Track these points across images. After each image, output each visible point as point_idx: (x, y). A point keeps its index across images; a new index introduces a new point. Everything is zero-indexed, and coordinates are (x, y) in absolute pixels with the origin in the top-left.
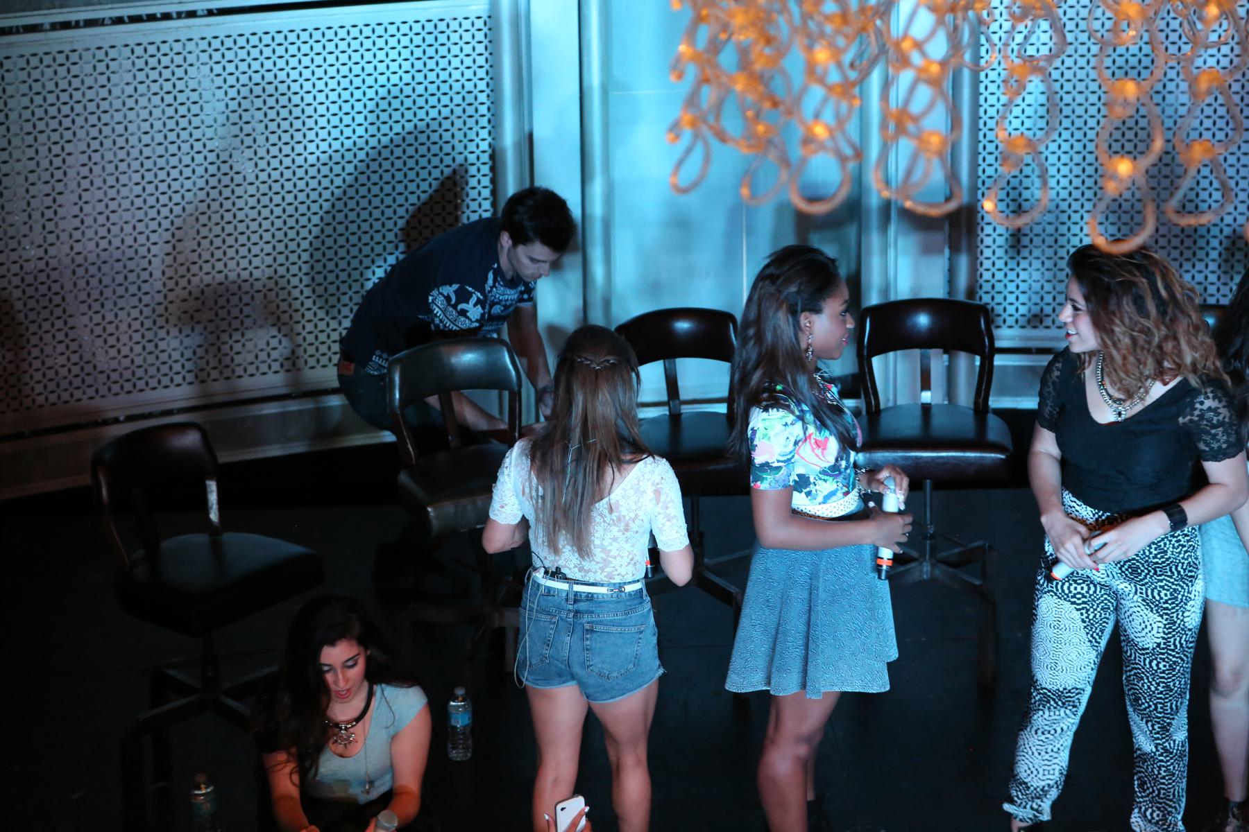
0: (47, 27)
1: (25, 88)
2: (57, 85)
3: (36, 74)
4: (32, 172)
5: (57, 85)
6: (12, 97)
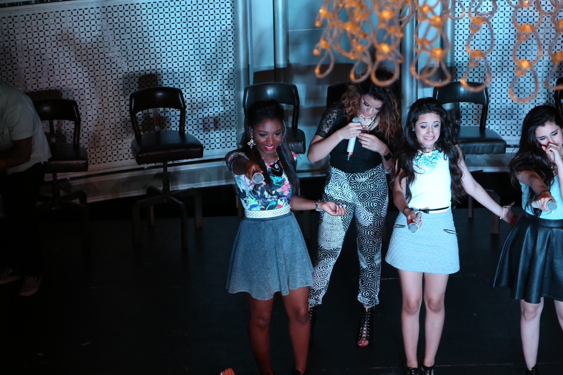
1: (23, 30)
2: (38, 29)
3: (28, 24)
4: (27, 68)
5: (38, 29)
6: (18, 34)
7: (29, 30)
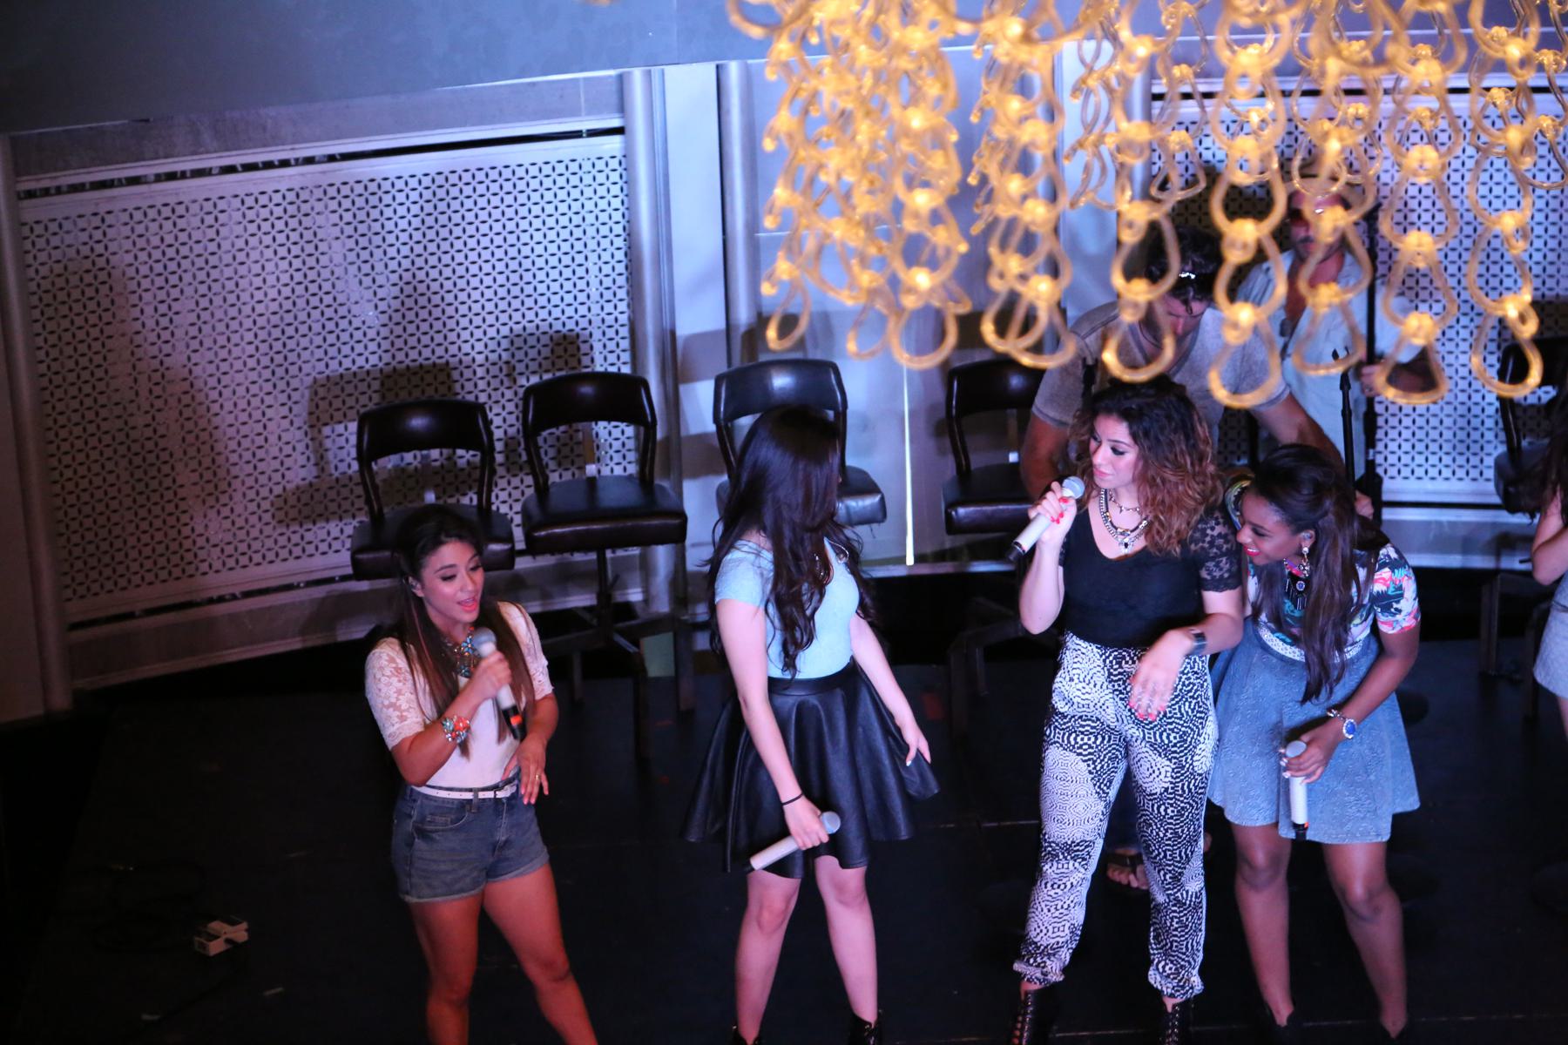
0: (152, 178)
1: (128, 245)
2: (162, 240)
3: (140, 229)
5: (162, 240)
7: (141, 243)
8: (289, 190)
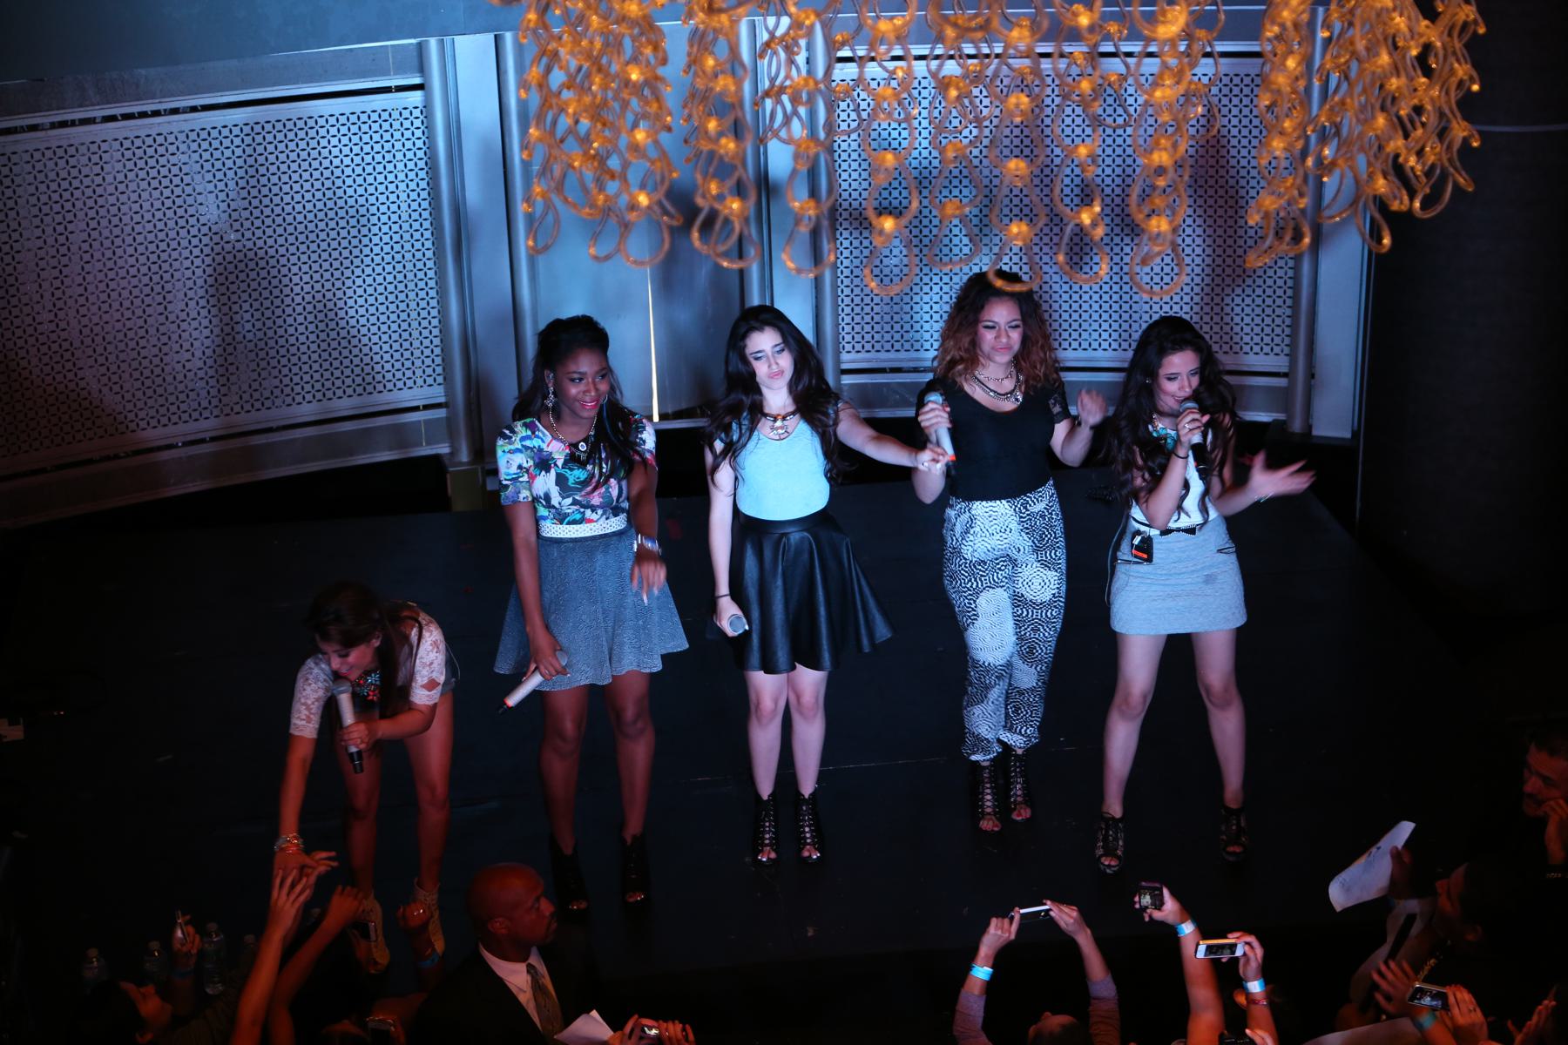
1: (30, 178)
2: (58, 174)
3: (39, 166)
4: (40, 248)
5: (58, 174)
7: (41, 177)
8: (1204, 75)
